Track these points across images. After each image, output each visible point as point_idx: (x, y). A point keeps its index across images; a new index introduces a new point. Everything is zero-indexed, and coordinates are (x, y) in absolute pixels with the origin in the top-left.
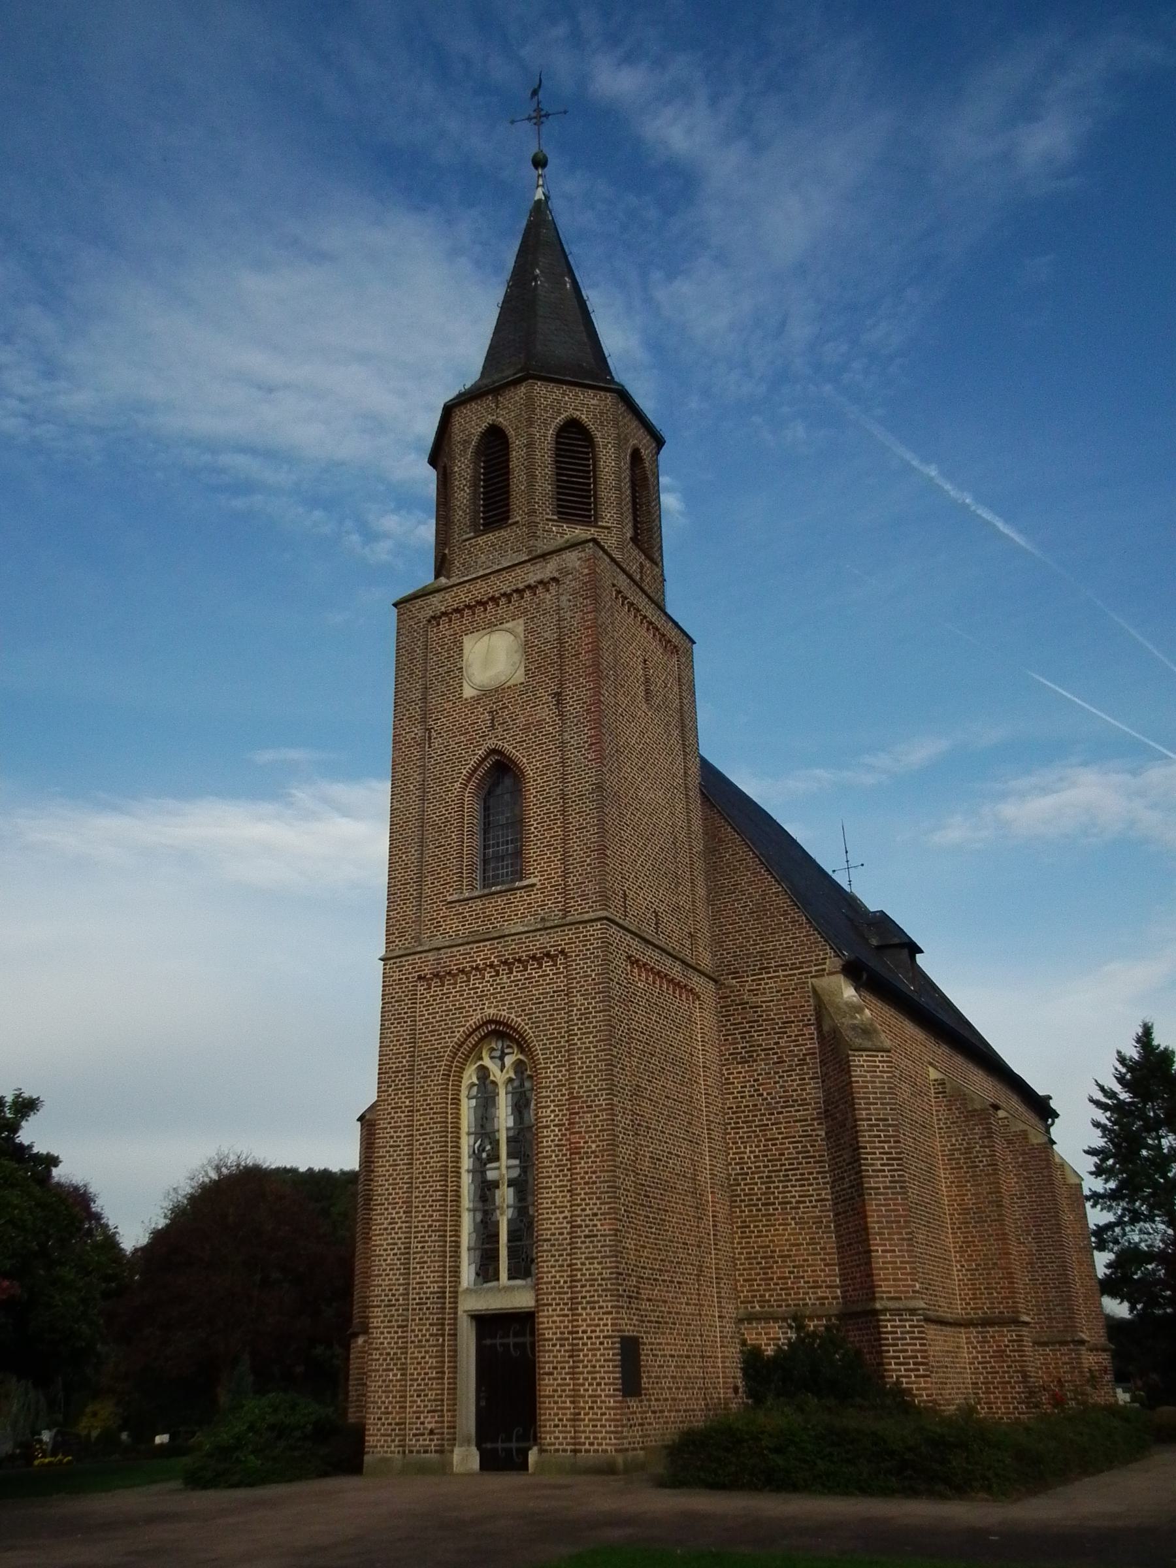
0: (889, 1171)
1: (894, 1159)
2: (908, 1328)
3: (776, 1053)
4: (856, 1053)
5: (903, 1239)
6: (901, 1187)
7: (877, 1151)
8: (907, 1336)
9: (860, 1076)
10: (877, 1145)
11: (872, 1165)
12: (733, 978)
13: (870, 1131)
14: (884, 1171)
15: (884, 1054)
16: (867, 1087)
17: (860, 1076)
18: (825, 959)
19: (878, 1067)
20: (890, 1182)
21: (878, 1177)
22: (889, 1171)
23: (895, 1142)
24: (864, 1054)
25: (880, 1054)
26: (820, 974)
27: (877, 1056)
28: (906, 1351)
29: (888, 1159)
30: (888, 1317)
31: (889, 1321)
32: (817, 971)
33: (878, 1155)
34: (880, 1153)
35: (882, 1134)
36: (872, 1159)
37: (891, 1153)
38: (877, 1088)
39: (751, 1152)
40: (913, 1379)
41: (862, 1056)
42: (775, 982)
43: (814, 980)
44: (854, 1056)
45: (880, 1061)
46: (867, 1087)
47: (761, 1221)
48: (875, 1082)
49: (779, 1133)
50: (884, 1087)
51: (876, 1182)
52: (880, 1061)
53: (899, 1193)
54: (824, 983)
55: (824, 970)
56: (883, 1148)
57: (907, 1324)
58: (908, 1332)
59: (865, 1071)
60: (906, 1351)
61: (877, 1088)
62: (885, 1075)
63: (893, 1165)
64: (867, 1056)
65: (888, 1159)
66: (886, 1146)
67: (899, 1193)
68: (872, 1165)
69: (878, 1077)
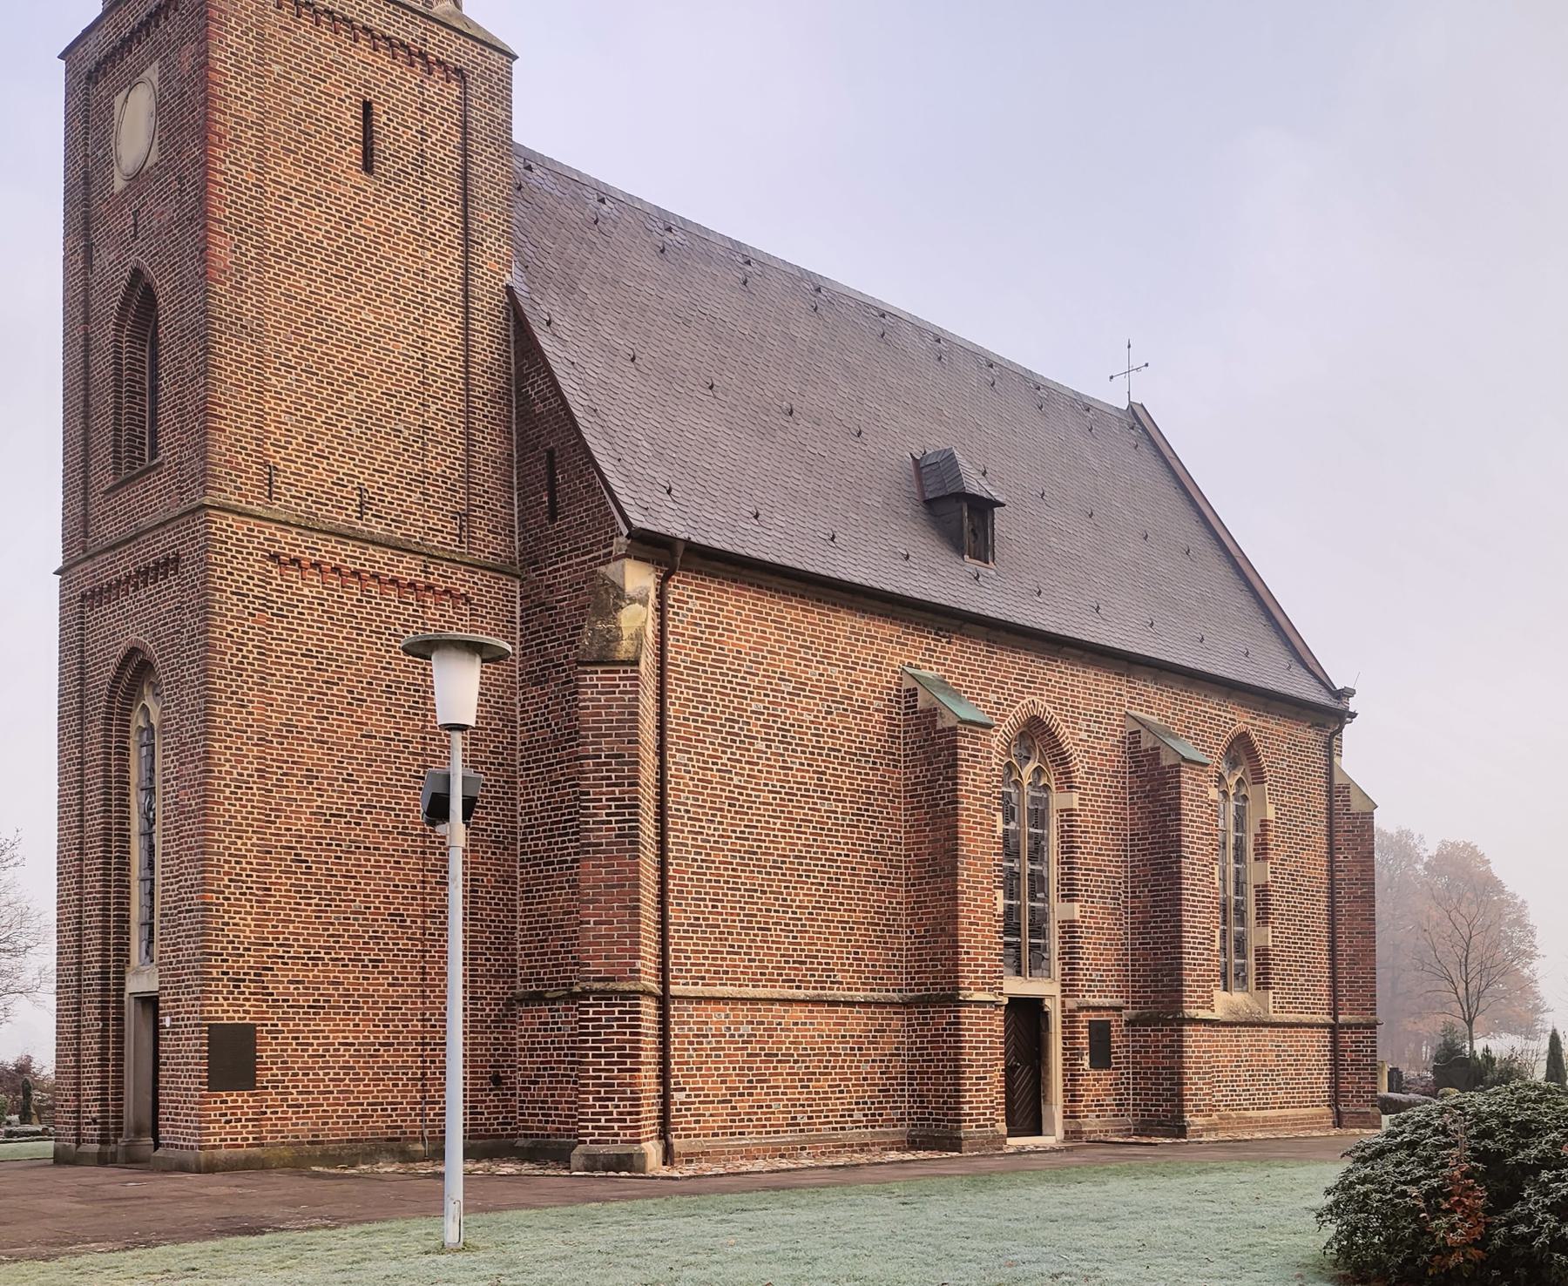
0: (617, 822)
1: (626, 807)
2: (617, 1015)
3: (564, 671)
4: (589, 669)
5: (626, 908)
6: (631, 843)
7: (604, 797)
8: (615, 1024)
9: (591, 700)
10: (604, 789)
11: (596, 815)
12: (534, 570)
13: (596, 771)
14: (610, 822)
15: (629, 669)
16: (599, 714)
17: (591, 700)
18: (612, 538)
19: (618, 686)
20: (617, 836)
21: (600, 830)
22: (617, 822)
23: (630, 785)
24: (599, 669)
25: (622, 669)
26: (608, 559)
27: (618, 672)
28: (612, 1041)
29: (617, 807)
30: (591, 1001)
31: (591, 1006)
32: (605, 555)
33: (604, 803)
34: (607, 800)
35: (613, 775)
36: (594, 808)
37: (624, 799)
38: (613, 714)
39: (540, 798)
40: (616, 1073)
41: (596, 672)
42: (569, 573)
43: (602, 569)
44: (586, 672)
45: (621, 679)
46: (599, 714)
47: (542, 884)
48: (611, 707)
49: (563, 775)
50: (623, 713)
51: (598, 837)
52: (621, 679)
53: (627, 851)
54: (610, 570)
55: (611, 553)
56: (613, 792)
57: (616, 1009)
58: (617, 1019)
59: (598, 693)
60: (612, 1041)
61: (613, 714)
62: (626, 697)
63: (624, 814)
64: (602, 672)
65: (617, 807)
66: (617, 790)
67: (627, 851)
68: (596, 815)
69: (616, 699)
